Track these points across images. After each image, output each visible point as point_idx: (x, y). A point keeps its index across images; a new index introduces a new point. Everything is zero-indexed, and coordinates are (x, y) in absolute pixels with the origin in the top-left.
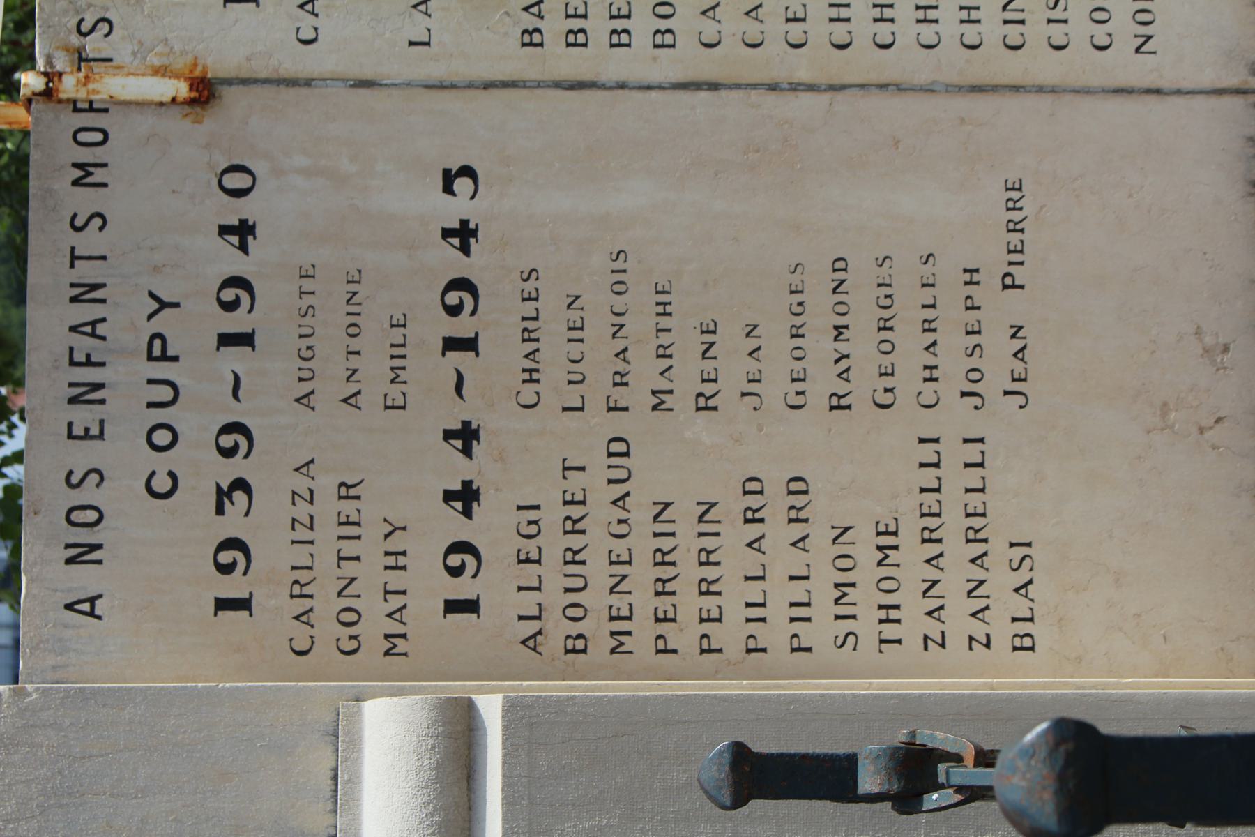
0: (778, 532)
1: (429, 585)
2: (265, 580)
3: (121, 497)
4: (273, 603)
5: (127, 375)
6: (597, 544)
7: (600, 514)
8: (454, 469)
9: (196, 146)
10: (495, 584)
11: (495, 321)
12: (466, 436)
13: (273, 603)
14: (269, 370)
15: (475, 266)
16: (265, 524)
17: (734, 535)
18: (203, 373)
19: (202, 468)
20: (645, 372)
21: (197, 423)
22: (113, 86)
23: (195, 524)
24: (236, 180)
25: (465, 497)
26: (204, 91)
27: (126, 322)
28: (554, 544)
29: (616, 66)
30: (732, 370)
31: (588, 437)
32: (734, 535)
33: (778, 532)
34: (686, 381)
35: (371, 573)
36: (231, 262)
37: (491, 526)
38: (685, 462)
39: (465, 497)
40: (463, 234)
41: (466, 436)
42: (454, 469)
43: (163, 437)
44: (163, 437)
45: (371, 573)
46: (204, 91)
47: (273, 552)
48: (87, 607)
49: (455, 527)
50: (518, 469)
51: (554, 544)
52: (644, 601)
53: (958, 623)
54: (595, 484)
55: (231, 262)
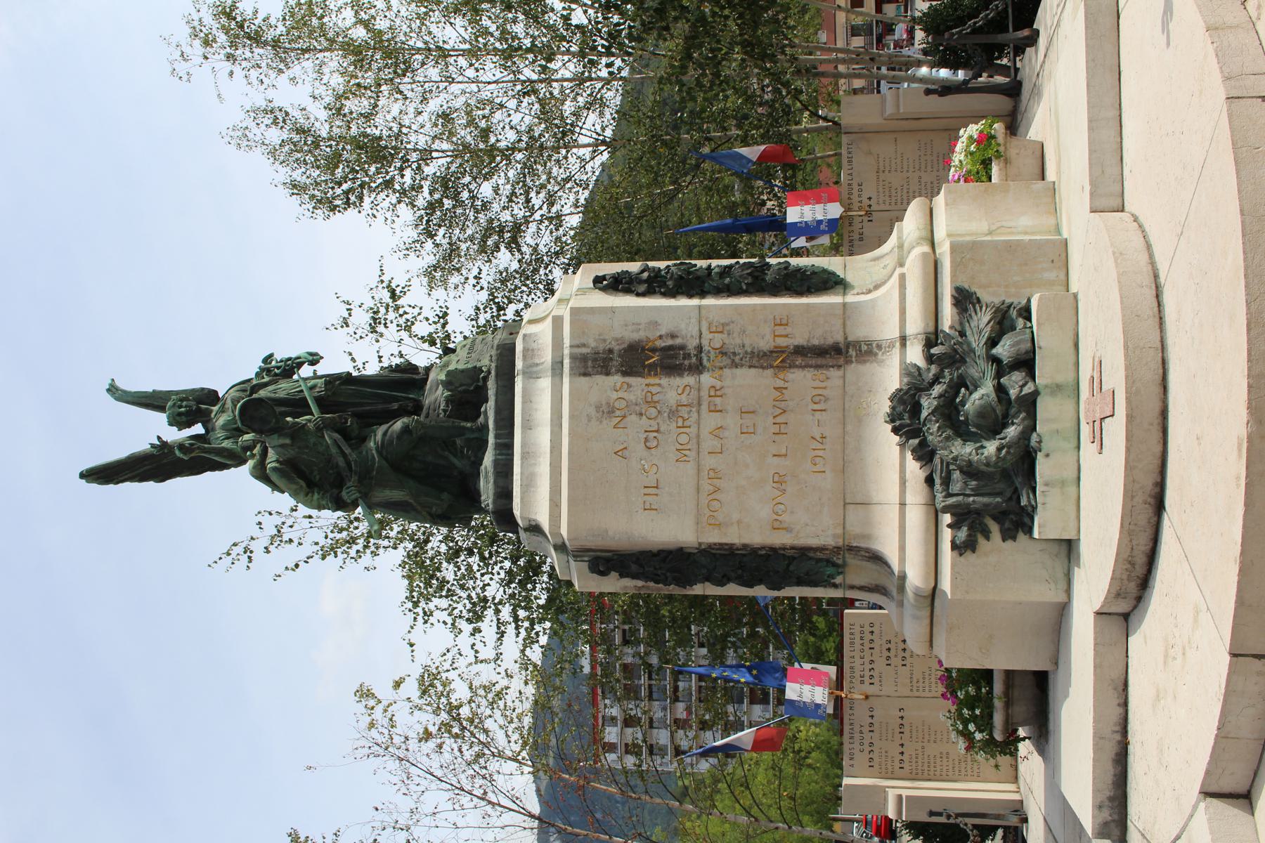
0: (945, 760)
1: (897, 765)
3: (856, 752)
4: (877, 766)
5: (857, 736)
6: (920, 760)
7: (920, 757)
11: (906, 729)
12: (902, 745)
13: (877, 766)
14: (876, 735)
15: (904, 722)
16: (875, 756)
17: (938, 760)
19: (867, 748)
20: (927, 737)
21: (866, 742)
23: (866, 756)
24: (871, 710)
25: (902, 753)
27: (857, 728)
28: (914, 760)
29: (923, 694)
32: (938, 760)
33: (945, 760)
34: (932, 738)
35: (889, 763)
36: (870, 720)
37: (905, 757)
39: (902, 753)
40: (902, 718)
41: (902, 745)
45: (889, 763)
46: (867, 697)
47: (876, 760)
48: (852, 766)
49: (900, 757)
50: (909, 750)
51: (914, 760)
52: (926, 768)
53: (969, 772)
54: (920, 752)
55: (870, 720)
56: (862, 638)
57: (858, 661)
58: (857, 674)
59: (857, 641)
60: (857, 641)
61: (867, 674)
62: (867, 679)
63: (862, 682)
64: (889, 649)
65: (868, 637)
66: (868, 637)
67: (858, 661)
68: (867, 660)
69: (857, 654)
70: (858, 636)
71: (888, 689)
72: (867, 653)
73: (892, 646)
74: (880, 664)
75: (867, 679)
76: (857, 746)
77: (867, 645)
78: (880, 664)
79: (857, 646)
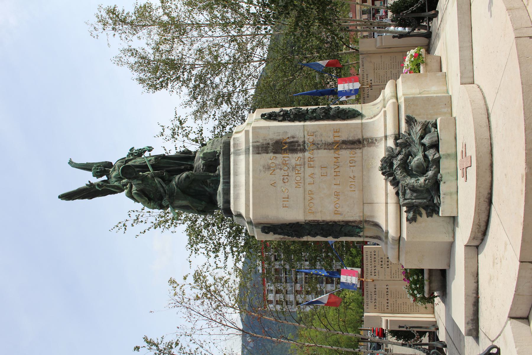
1: (386, 307)
2: (377, 307)
3: (369, 302)
5: (369, 296)
6: (395, 306)
7: (395, 304)
8: (387, 301)
9: (373, 283)
10: (389, 307)
11: (389, 293)
16: (377, 304)
18: (374, 296)
20: (397, 296)
21: (373, 299)
22: (368, 280)
23: (373, 304)
24: (375, 286)
26: (373, 281)
27: (369, 293)
30: (402, 296)
31: (394, 300)
35: (383, 307)
37: (389, 304)
38: (400, 301)
42: (387, 301)
43: (371, 299)
44: (371, 299)
47: (377, 306)
56: (371, 257)
57: (369, 266)
58: (369, 271)
59: (369, 258)
60: (369, 258)
61: (373, 271)
62: (373, 274)
63: (371, 275)
64: (382, 261)
65: (373, 256)
66: (373, 256)
67: (369, 266)
68: (373, 266)
69: (369, 263)
70: (369, 256)
71: (381, 277)
72: (373, 263)
73: (383, 260)
74: (378, 267)
75: (373, 274)
76: (369, 300)
77: (373, 258)
78: (378, 267)
79: (369, 260)
